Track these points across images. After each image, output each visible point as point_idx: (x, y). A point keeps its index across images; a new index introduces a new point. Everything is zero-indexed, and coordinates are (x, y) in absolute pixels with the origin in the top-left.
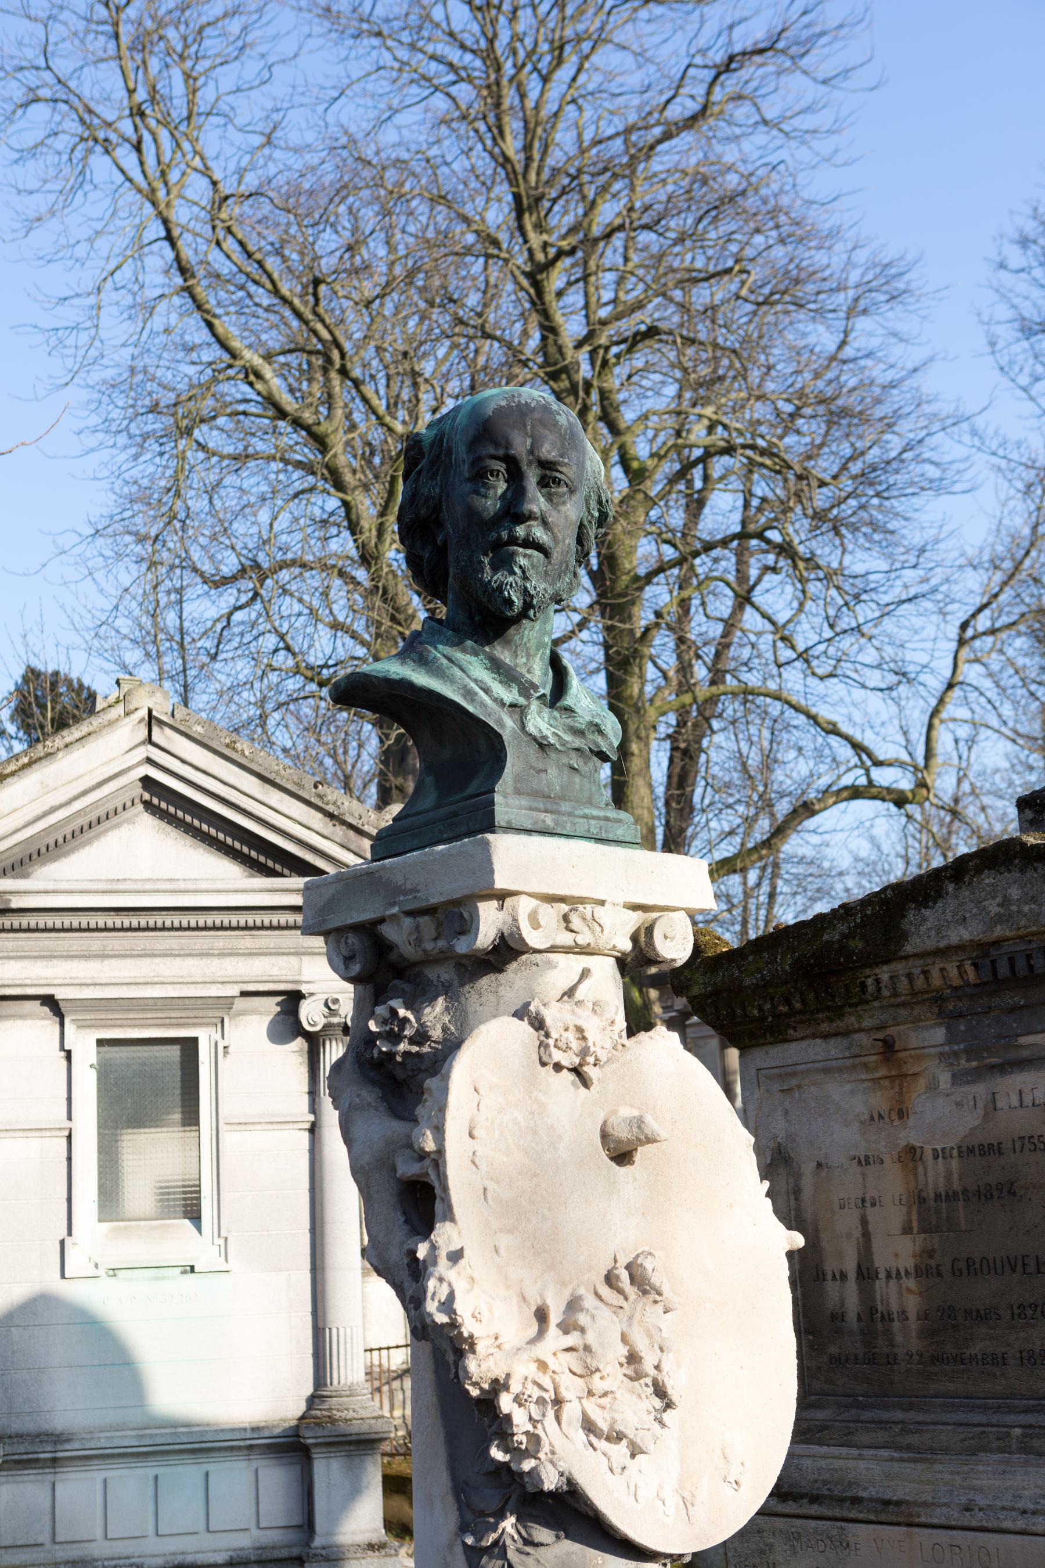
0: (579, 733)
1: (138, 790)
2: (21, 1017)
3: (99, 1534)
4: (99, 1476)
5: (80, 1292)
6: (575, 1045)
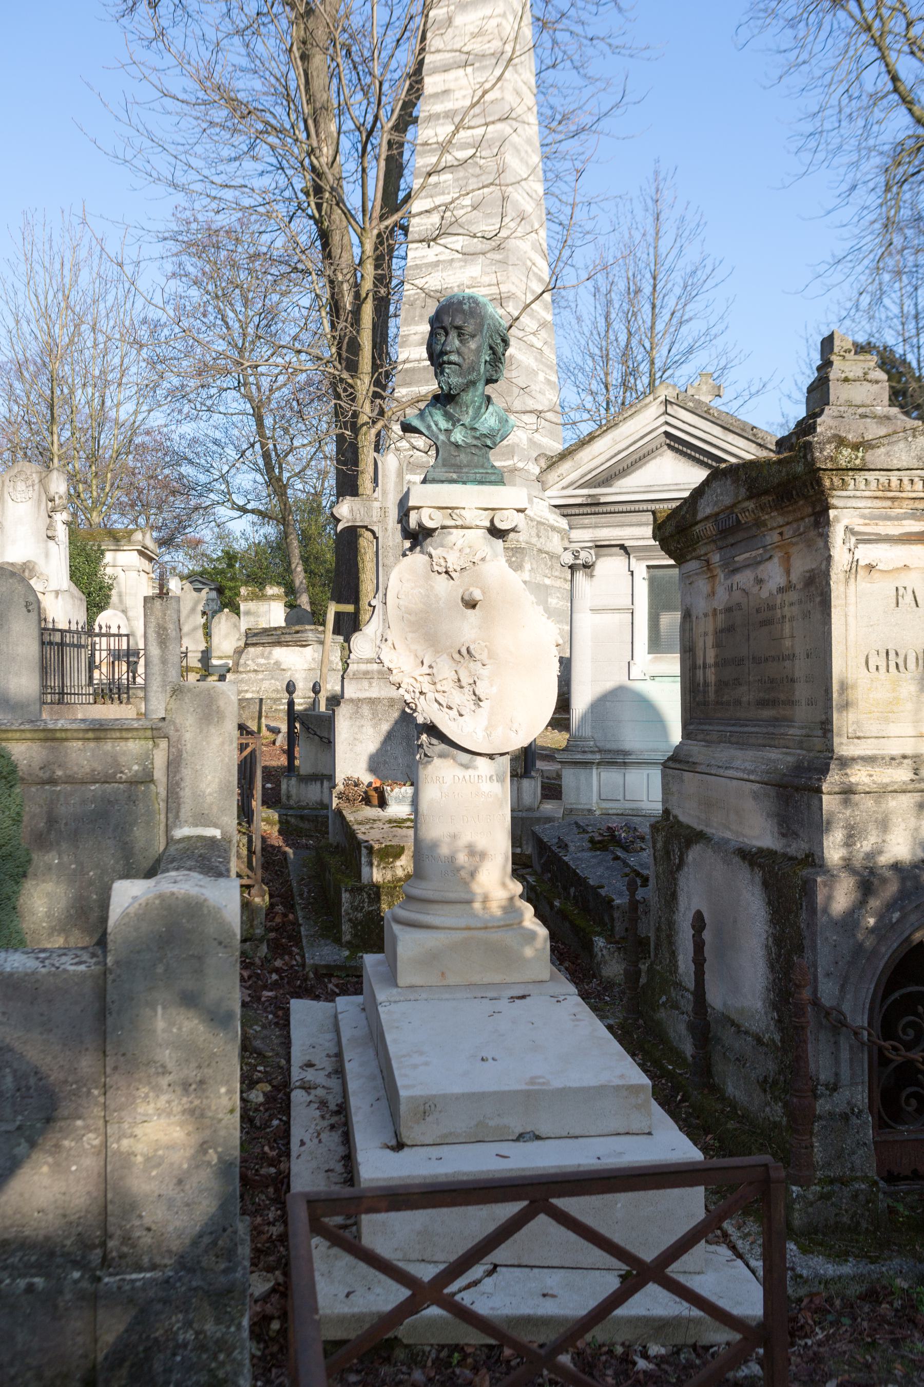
0: (477, 438)
1: (663, 438)
2: (611, 555)
3: (645, 798)
4: (646, 772)
5: (639, 686)
6: (443, 564)
